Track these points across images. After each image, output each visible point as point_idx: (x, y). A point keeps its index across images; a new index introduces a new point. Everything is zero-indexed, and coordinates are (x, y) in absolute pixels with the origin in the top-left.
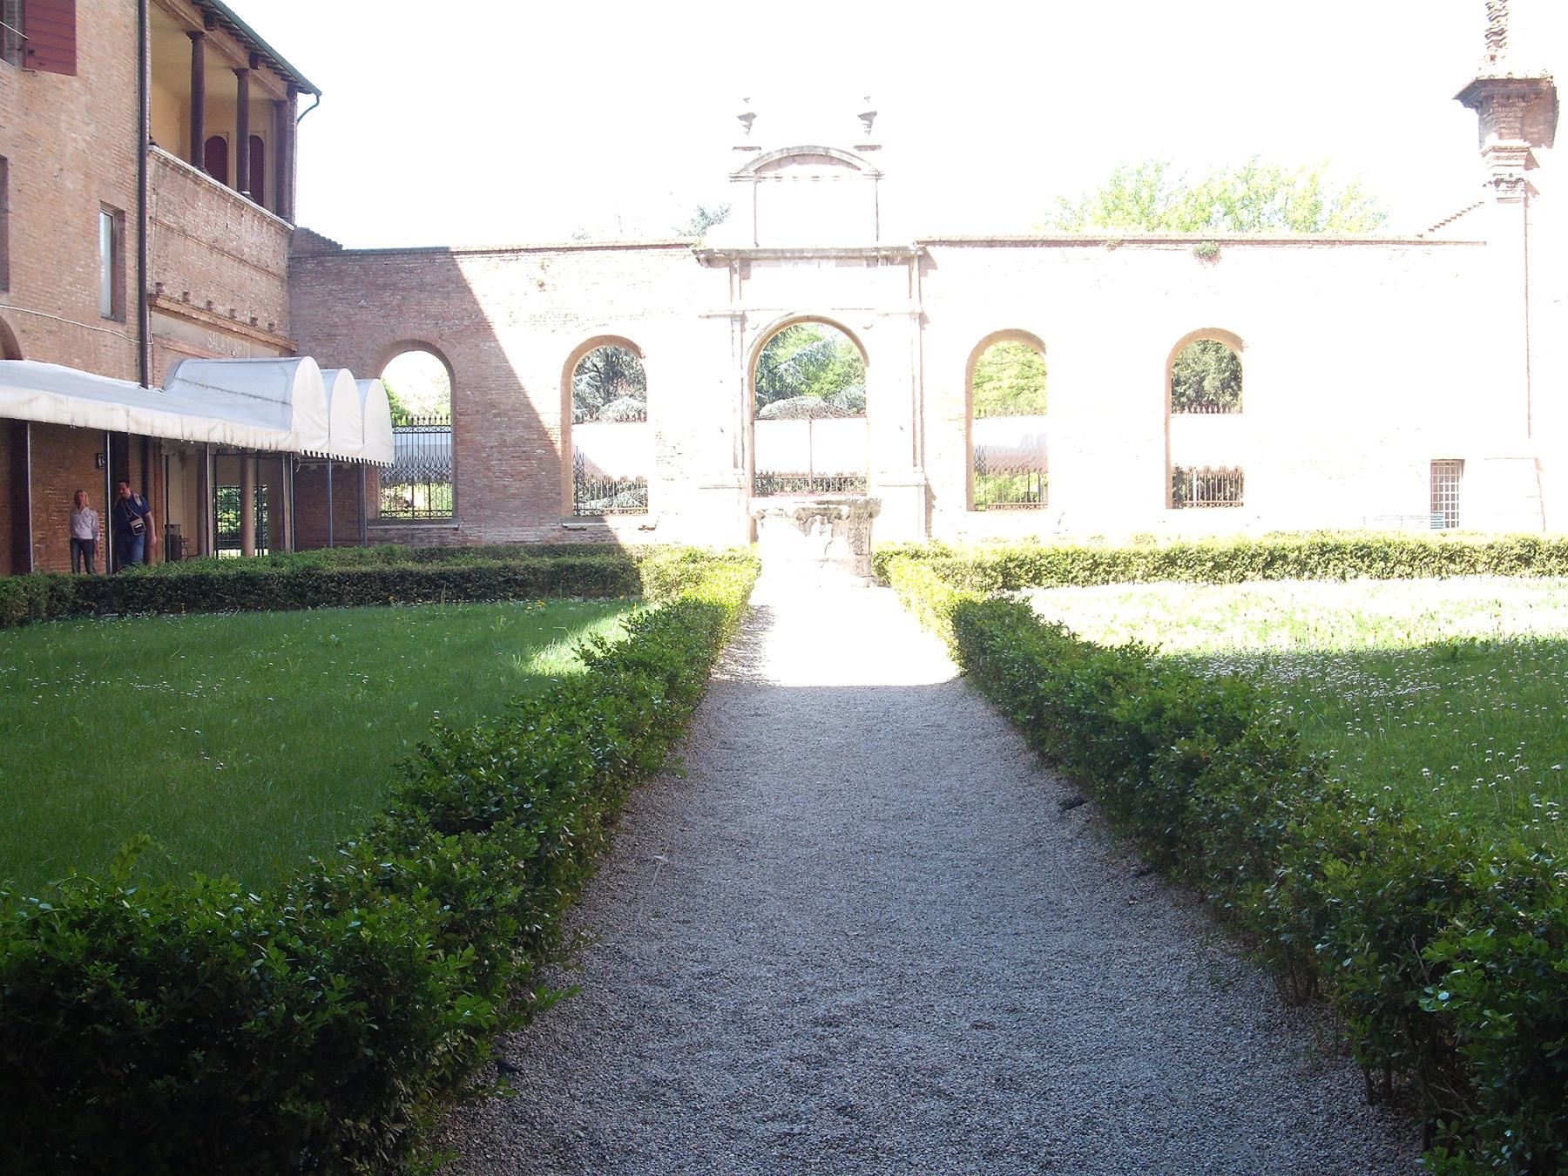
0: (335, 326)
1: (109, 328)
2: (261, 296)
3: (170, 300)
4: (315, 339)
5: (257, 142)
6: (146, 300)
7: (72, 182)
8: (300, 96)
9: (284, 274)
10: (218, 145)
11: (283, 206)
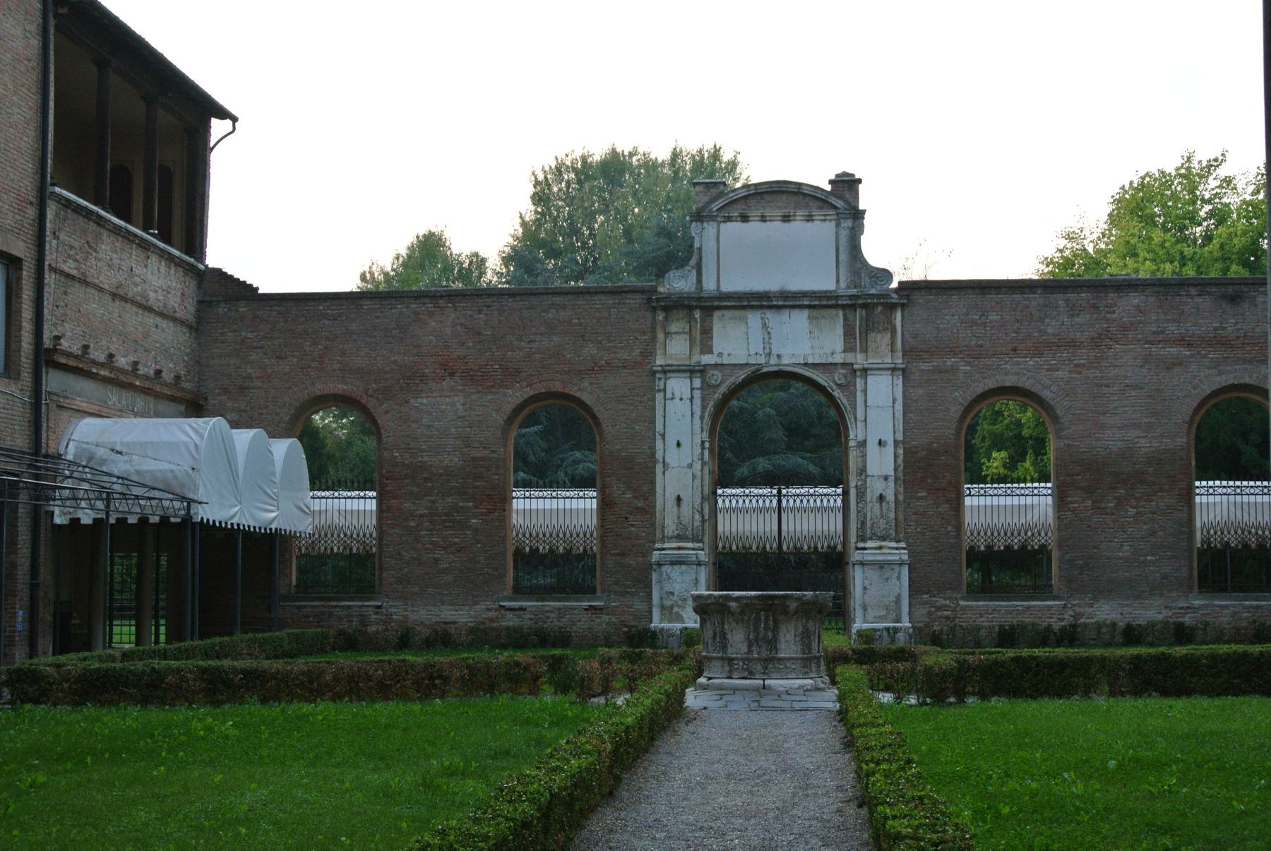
0: (249, 377)
3: (69, 355)
4: (225, 391)
6: (46, 358)
8: (215, 122)
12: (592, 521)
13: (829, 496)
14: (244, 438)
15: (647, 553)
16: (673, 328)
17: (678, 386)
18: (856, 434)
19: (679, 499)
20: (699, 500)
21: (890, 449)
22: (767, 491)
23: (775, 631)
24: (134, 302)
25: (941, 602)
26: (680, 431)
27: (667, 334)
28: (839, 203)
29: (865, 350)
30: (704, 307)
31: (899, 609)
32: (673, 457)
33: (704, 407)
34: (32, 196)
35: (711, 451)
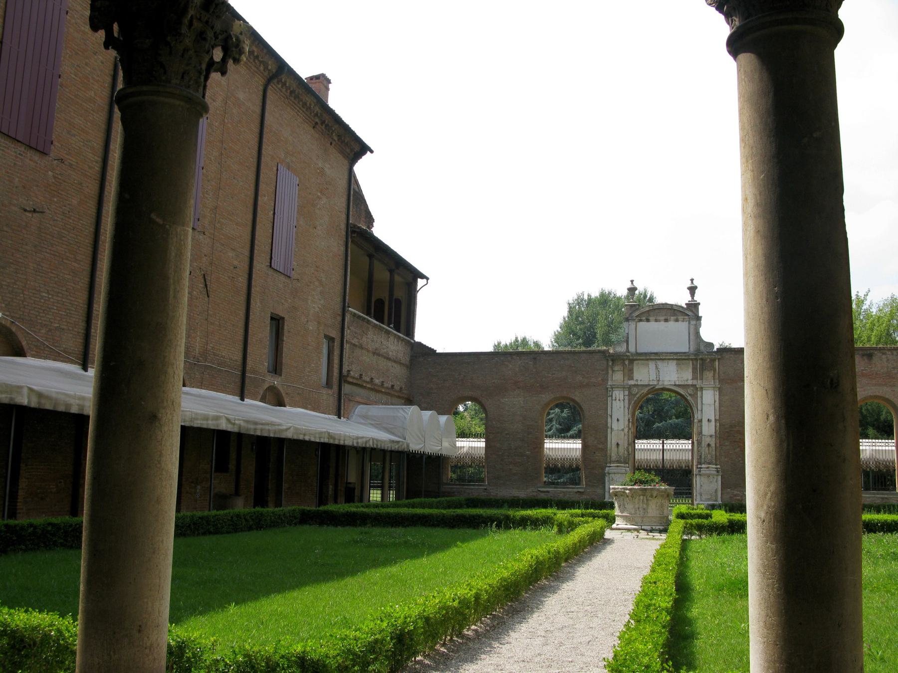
1: (325, 391)
2: (396, 375)
3: (353, 378)
5: (398, 302)
7: (311, 327)
9: (408, 363)
10: (380, 303)
11: (409, 330)
12: (578, 454)
13: (685, 445)
14: (427, 414)
15: (603, 469)
16: (616, 368)
17: (618, 394)
18: (697, 416)
19: (618, 444)
20: (626, 445)
21: (713, 423)
22: (657, 441)
23: (648, 505)
24: (382, 356)
25: (736, 492)
26: (619, 415)
27: (613, 371)
28: (690, 313)
29: (702, 379)
30: (628, 361)
31: (716, 496)
32: (615, 426)
33: (629, 404)
34: (340, 312)
35: (633, 423)
